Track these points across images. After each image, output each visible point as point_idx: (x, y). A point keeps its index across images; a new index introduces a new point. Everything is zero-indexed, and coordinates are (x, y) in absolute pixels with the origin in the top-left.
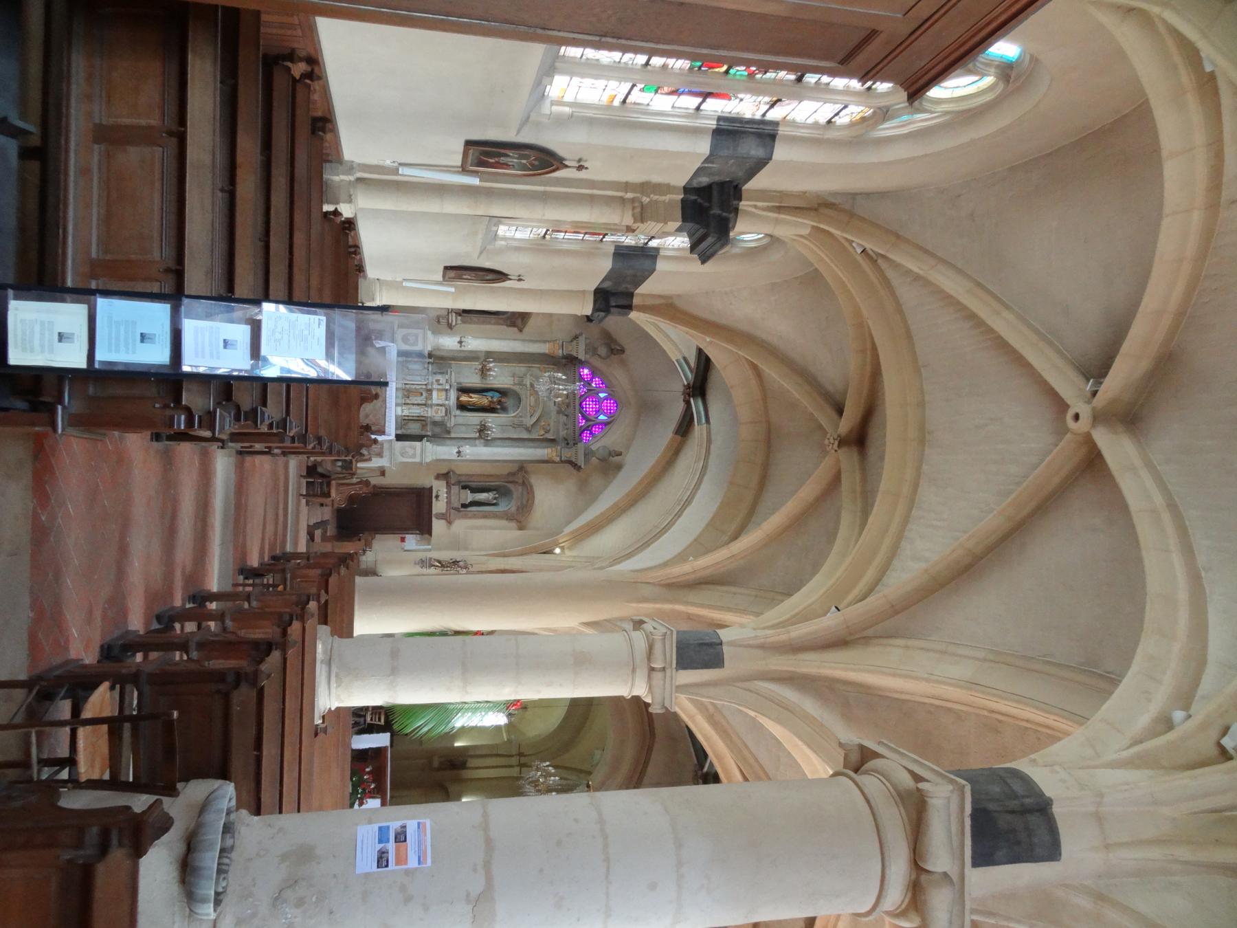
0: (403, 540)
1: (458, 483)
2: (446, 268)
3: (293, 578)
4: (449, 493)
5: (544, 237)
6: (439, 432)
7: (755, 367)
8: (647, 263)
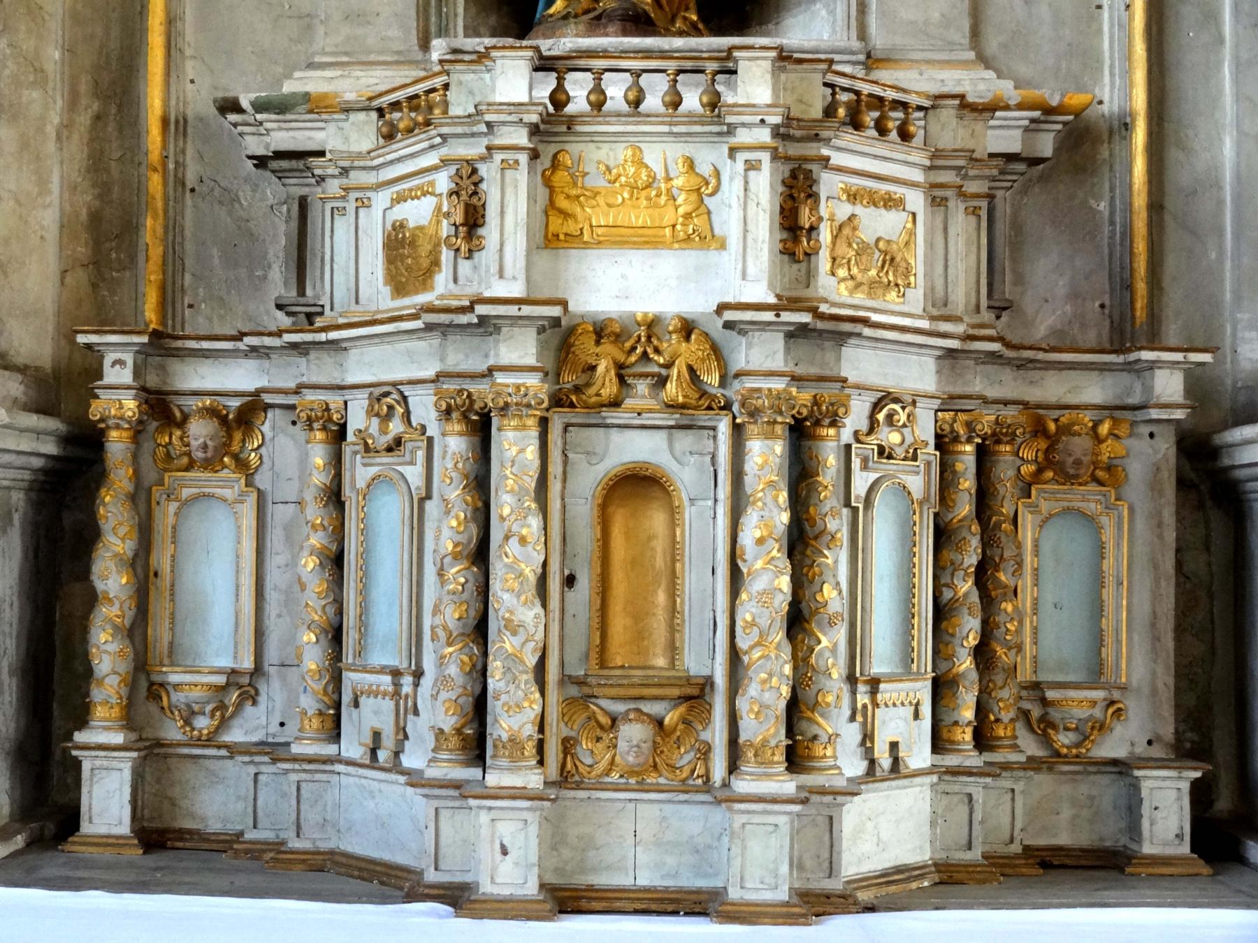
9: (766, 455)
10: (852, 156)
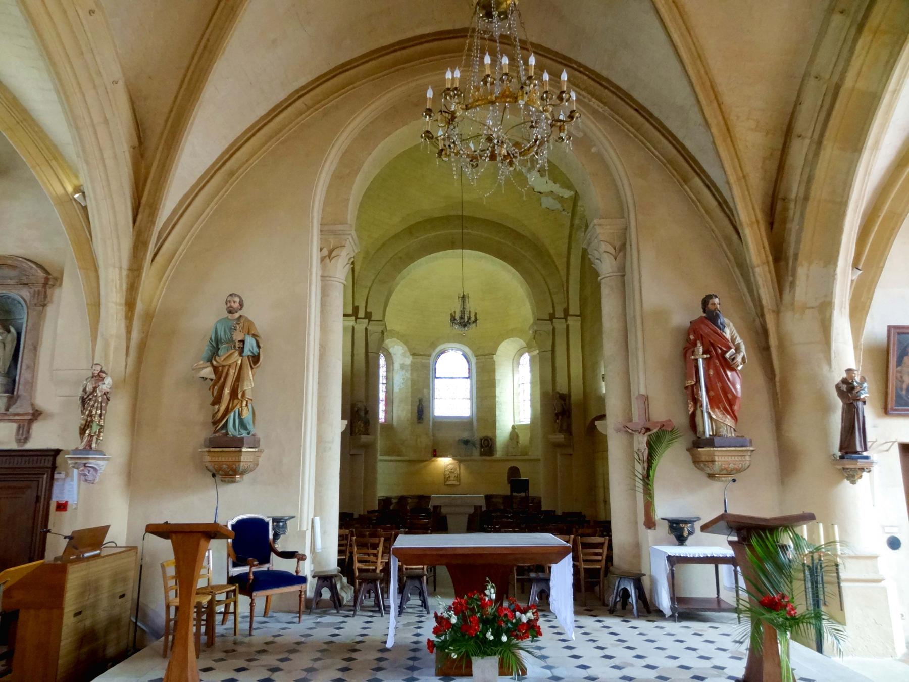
0: (62, 507)
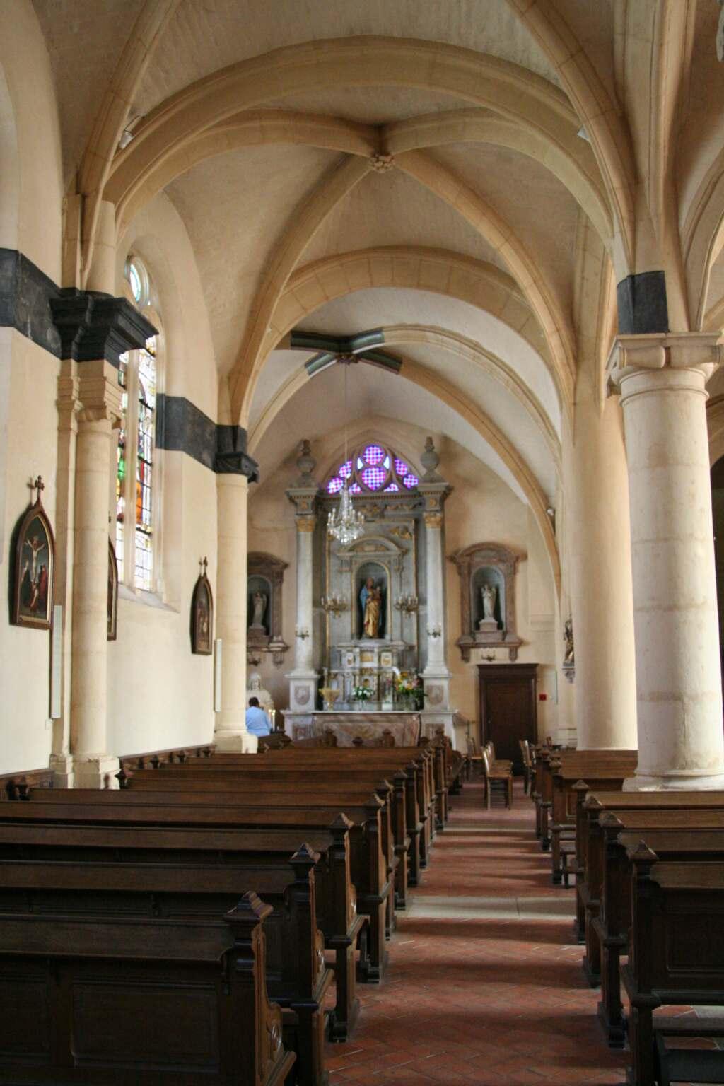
1: (472, 634)
2: (194, 650)
3: (565, 822)
4: (485, 645)
5: (149, 534)
6: (412, 658)
7: (299, 272)
8: (175, 407)
9: (376, 678)
10: (384, 654)
